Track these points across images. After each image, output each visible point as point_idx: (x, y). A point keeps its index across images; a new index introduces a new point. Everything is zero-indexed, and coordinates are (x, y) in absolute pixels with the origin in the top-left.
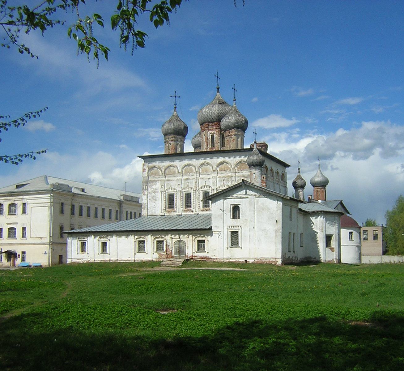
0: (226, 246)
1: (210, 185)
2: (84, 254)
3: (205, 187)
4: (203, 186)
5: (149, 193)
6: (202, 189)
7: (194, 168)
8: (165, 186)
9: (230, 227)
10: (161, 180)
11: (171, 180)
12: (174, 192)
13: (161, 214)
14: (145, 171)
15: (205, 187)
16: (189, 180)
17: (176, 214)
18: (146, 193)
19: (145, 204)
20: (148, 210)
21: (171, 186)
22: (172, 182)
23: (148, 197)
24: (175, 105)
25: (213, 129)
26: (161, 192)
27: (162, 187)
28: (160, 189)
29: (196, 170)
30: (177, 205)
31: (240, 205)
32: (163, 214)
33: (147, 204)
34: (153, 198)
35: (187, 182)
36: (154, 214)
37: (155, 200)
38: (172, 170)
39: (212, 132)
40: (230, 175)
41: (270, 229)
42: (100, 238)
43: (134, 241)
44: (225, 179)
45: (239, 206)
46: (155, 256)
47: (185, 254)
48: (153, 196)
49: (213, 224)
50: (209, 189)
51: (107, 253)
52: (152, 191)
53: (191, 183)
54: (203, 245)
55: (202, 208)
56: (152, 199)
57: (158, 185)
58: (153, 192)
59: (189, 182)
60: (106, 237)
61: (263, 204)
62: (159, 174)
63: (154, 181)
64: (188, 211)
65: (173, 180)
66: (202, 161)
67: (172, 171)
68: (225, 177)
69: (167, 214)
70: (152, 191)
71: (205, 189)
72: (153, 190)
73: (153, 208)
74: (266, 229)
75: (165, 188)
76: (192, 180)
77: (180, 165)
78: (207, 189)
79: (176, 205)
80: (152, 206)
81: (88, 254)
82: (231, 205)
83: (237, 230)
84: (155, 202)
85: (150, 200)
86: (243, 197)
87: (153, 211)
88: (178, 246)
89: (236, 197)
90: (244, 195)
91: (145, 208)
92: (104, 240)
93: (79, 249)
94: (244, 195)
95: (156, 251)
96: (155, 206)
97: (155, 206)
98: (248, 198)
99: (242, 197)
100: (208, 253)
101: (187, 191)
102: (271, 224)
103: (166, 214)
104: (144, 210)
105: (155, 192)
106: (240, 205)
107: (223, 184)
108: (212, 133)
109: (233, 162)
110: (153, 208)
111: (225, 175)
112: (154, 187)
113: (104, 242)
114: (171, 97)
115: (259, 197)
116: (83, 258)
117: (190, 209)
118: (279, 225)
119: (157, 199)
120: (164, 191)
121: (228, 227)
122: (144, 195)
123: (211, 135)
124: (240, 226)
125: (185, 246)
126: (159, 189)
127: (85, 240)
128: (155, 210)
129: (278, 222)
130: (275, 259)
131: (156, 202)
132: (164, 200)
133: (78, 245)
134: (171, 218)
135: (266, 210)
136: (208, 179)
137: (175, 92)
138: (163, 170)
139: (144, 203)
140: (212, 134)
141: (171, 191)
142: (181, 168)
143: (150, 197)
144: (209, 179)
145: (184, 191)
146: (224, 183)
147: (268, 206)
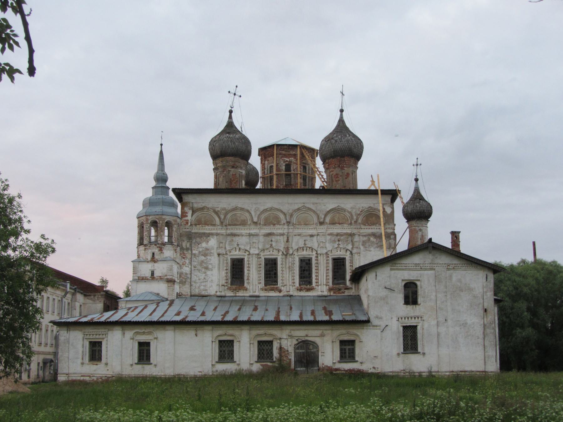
0: (395, 352)
1: (313, 247)
2: (97, 364)
3: (303, 250)
4: (300, 248)
5: (193, 256)
6: (299, 253)
7: (282, 216)
8: (226, 245)
9: (402, 318)
10: (217, 234)
11: (239, 235)
12: (245, 256)
13: (218, 294)
15: (305, 251)
16: (273, 237)
17: (248, 295)
18: (189, 256)
19: (186, 274)
20: (191, 285)
21: (238, 245)
22: (240, 237)
23: (192, 262)
24: (232, 108)
25: (289, 155)
26: (219, 255)
27: (219, 245)
28: (215, 249)
29: (286, 220)
30: (251, 279)
31: (419, 280)
32: (223, 294)
33: (189, 276)
35: (269, 238)
37: (207, 268)
38: (240, 217)
39: (288, 160)
40: (349, 231)
41: (473, 323)
43: (212, 342)
44: (342, 238)
45: (418, 283)
47: (318, 366)
48: (202, 262)
49: (372, 313)
50: (311, 253)
51: (151, 364)
52: (200, 252)
53: (277, 242)
54: (349, 349)
55: (297, 284)
56: (199, 267)
57: (213, 242)
58: (202, 255)
59: (273, 240)
60: (150, 333)
61: (460, 281)
62: (213, 223)
63: (204, 234)
64: (272, 290)
65: (243, 236)
67: (238, 218)
68: (342, 235)
69: (229, 294)
70: (200, 252)
71: (305, 253)
72: (201, 250)
73: (201, 282)
74: (466, 324)
75: (225, 248)
76: (278, 237)
78: (308, 253)
79: (248, 279)
81: (107, 364)
82: (403, 280)
83: (415, 324)
84: (205, 273)
85: (195, 267)
86: (426, 268)
87: (202, 287)
89: (412, 268)
91: (185, 282)
93: (86, 354)
95: (256, 360)
97: (205, 278)
99: (424, 267)
100: (361, 363)
101: (269, 254)
102: (475, 315)
103: (261, 295)
104: (184, 285)
105: (205, 255)
106: (419, 280)
107: (336, 246)
108: (287, 161)
109: (354, 211)
110: (201, 282)
111: (341, 231)
112: (204, 245)
113: (95, 342)
114: (229, 92)
115: (454, 268)
116: (95, 372)
117: (276, 286)
118: (490, 317)
119: (210, 266)
120: (225, 253)
121: (399, 318)
122: (184, 258)
123: (284, 164)
124: (421, 317)
126: (213, 249)
127: (101, 337)
128: (205, 286)
129: (488, 312)
130: (484, 373)
131: (209, 273)
132: (225, 268)
133: (83, 347)
136: (309, 237)
137: (237, 87)
138: (222, 217)
140: (287, 163)
141: (237, 254)
142: (257, 216)
143: (195, 264)
144: (312, 236)
145: (264, 256)
146: (339, 244)
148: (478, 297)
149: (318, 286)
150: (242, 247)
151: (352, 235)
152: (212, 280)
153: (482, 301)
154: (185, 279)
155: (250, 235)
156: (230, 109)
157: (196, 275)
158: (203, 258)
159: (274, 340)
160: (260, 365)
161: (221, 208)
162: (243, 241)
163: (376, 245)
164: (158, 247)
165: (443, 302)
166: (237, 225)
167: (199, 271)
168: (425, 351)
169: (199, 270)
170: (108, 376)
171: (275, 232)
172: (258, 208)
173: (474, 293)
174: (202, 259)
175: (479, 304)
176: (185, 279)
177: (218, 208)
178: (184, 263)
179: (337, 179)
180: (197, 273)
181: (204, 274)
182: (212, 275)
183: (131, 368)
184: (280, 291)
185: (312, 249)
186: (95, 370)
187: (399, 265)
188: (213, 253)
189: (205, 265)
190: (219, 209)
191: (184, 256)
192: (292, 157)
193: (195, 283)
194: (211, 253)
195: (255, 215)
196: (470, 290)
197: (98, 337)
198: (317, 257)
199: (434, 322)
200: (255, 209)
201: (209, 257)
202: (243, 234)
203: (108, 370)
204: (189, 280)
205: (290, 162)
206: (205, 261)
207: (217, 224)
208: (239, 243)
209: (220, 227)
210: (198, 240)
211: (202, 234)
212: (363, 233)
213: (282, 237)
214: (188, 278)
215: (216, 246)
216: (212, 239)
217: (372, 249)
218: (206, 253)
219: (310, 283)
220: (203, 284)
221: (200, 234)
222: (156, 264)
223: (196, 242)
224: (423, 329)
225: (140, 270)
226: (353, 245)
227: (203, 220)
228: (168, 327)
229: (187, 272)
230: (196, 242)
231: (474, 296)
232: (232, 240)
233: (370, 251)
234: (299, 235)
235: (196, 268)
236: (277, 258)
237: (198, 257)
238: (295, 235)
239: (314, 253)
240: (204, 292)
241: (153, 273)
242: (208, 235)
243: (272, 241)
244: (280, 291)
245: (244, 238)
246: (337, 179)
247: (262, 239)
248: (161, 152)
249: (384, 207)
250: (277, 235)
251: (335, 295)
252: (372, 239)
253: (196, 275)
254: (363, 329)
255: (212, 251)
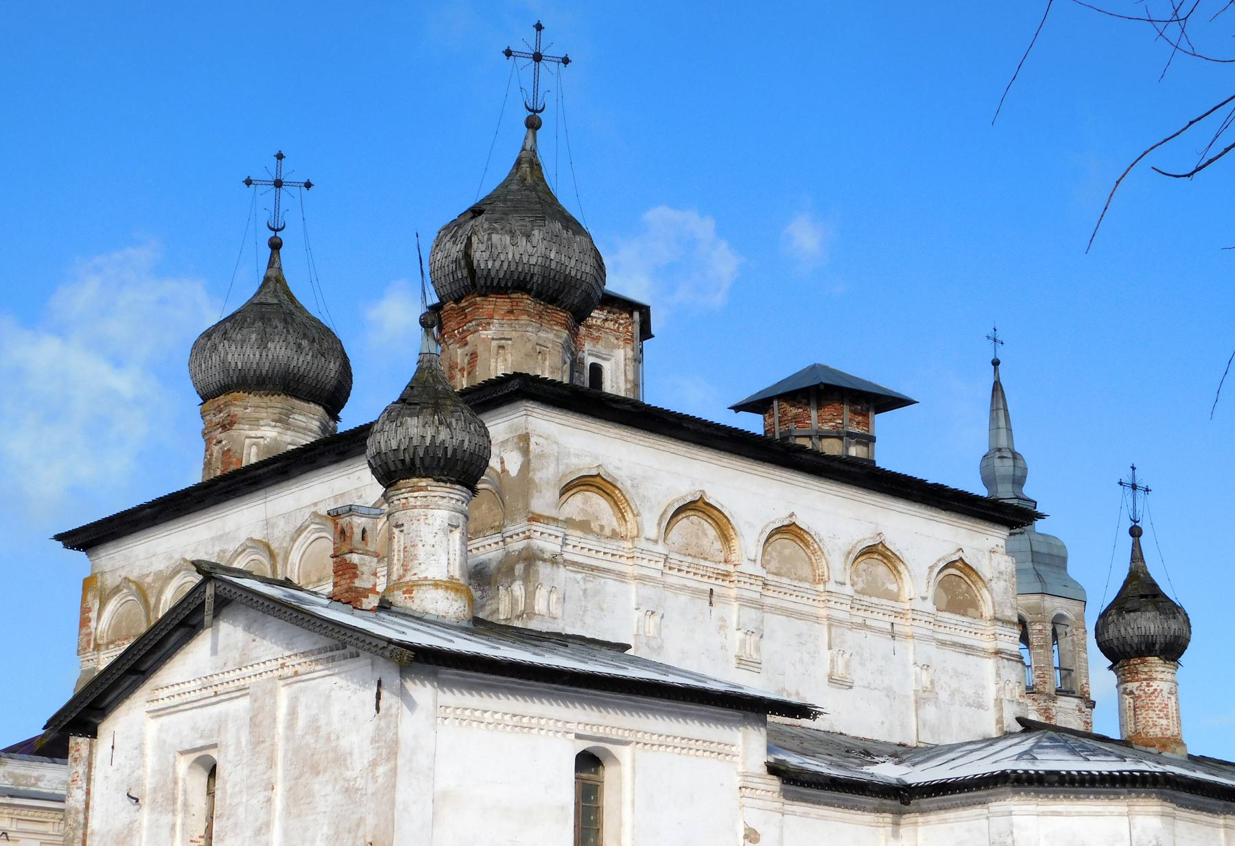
19: (77, 812)
31: (215, 746)
33: (81, 817)
61: (314, 727)
106: (215, 746)
115: (296, 674)
135: (325, 771)
147: (338, 738)
148: (357, 789)
156: (272, 234)
161: (155, 574)
165: (260, 830)
173: (348, 774)
177: (148, 575)
187: (166, 692)
190: (149, 580)
196: (340, 759)
204: (80, 833)
214: (79, 823)
231: (347, 790)
248: (997, 387)
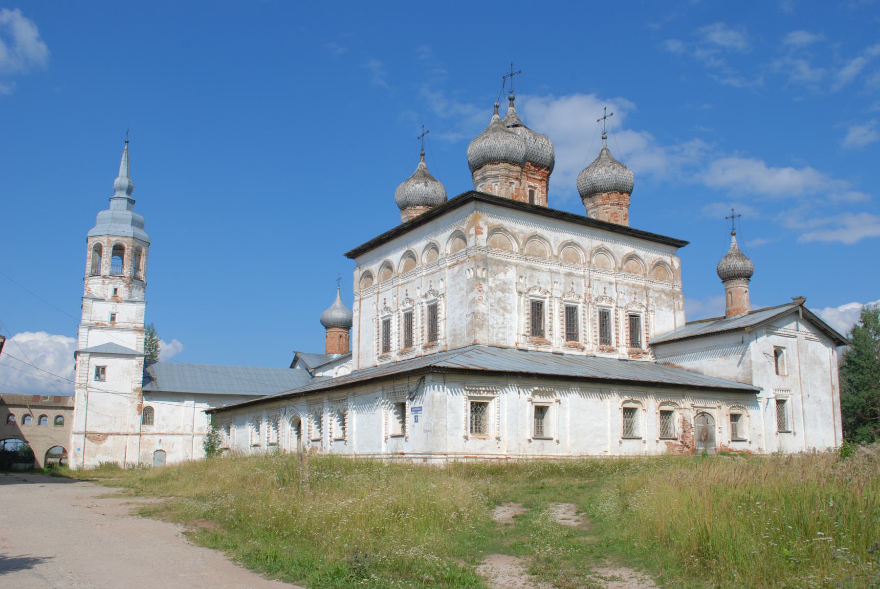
2: (484, 439)
10: (517, 265)
11: (539, 270)
14: (482, 233)
16: (575, 278)
17: (551, 350)
22: (540, 273)
25: (534, 179)
34: (498, 304)
35: (570, 279)
36: (502, 343)
37: (505, 309)
38: (538, 246)
39: (533, 185)
42: (535, 393)
44: (638, 290)
46: (661, 448)
48: (500, 299)
52: (496, 285)
53: (577, 285)
56: (496, 306)
57: (511, 275)
58: (500, 290)
60: (548, 394)
61: (813, 352)
63: (501, 261)
65: (543, 271)
66: (597, 243)
68: (637, 288)
70: (496, 285)
72: (498, 282)
73: (499, 328)
74: (821, 401)
76: (578, 280)
77: (556, 240)
80: (497, 324)
84: (503, 315)
87: (500, 335)
88: (702, 425)
90: (791, 331)
91: (482, 325)
92: (540, 400)
94: (791, 331)
96: (503, 323)
97: (503, 323)
98: (795, 337)
100: (750, 442)
104: (481, 329)
105: (503, 291)
108: (531, 186)
110: (499, 328)
112: (501, 276)
116: (484, 452)
119: (509, 307)
122: (480, 291)
123: (529, 189)
125: (714, 426)
131: (507, 315)
134: (573, 359)
136: (608, 284)
139: (481, 311)
140: (531, 189)
142: (557, 248)
149: (619, 347)
150: (543, 286)
151: (647, 289)
152: (511, 327)
153: (830, 377)
154: (482, 321)
155: (551, 272)
157: (493, 317)
158: (499, 294)
159: (676, 410)
160: (665, 442)
162: (544, 277)
163: (666, 305)
164: (123, 281)
166: (536, 256)
167: (496, 312)
168: (796, 431)
169: (497, 311)
170: (500, 457)
171: (574, 272)
172: (558, 238)
174: (500, 296)
175: (828, 380)
176: (482, 321)
177: (515, 228)
178: (481, 298)
179: (616, 219)
180: (494, 314)
181: (502, 317)
182: (511, 319)
183: (528, 445)
184: (583, 349)
185: (611, 300)
186: (482, 449)
188: (512, 290)
189: (503, 305)
190: (517, 231)
191: (480, 289)
192: (537, 183)
193: (493, 328)
194: (510, 289)
195: (555, 247)
197: (486, 395)
198: (616, 310)
199: (799, 397)
200: (554, 239)
201: (506, 294)
202: (543, 269)
203: (499, 448)
205: (535, 188)
206: (503, 299)
207: (514, 250)
208: (539, 281)
209: (519, 255)
210: (494, 268)
211: (498, 261)
212: (655, 288)
213: (583, 280)
215: (515, 281)
216: (510, 270)
217: (663, 308)
218: (504, 288)
219: (609, 343)
220: (500, 330)
221: (496, 260)
222: (119, 305)
223: (492, 271)
224: (792, 404)
225: (95, 311)
226: (648, 301)
227: (497, 242)
228: (574, 386)
229: (484, 311)
230: (492, 271)
232: (532, 275)
233: (662, 310)
234: (599, 280)
235: (493, 308)
236: (577, 306)
237: (495, 292)
238: (595, 280)
239: (614, 305)
240: (502, 342)
241: (113, 318)
242: (506, 264)
243: (573, 283)
244: (583, 349)
245: (544, 274)
246: (616, 219)
247: (562, 279)
249: (673, 260)
250: (578, 277)
251: (633, 359)
252: (663, 296)
253: (493, 317)
254: (749, 400)
255: (510, 287)
